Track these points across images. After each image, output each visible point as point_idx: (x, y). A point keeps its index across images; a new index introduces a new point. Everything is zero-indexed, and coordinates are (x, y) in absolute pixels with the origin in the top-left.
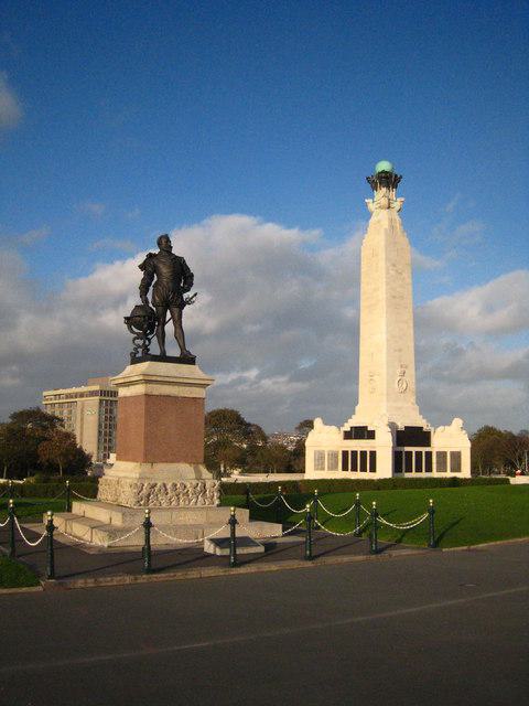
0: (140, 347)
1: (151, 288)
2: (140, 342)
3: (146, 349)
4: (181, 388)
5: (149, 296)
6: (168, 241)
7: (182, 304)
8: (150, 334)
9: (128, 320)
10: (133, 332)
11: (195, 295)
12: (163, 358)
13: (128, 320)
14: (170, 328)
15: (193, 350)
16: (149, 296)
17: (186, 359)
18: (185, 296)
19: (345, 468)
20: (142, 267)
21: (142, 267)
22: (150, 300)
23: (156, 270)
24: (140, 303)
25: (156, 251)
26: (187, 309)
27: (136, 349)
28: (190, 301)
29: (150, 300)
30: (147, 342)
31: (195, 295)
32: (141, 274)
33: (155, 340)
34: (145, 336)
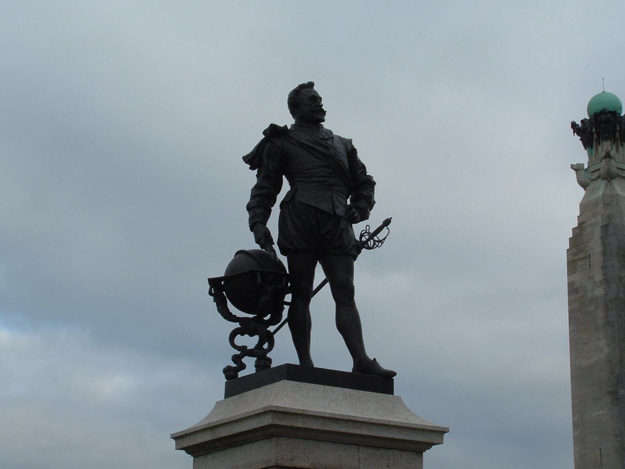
1: (276, 210)
2: (250, 341)
3: (260, 354)
5: (273, 225)
6: (316, 100)
8: (272, 322)
11: (387, 222)
12: (305, 372)
14: (323, 306)
16: (273, 225)
18: (358, 229)
20: (252, 160)
21: (252, 160)
22: (275, 234)
24: (250, 244)
25: (287, 120)
27: (236, 359)
28: (372, 240)
29: (275, 234)
30: (266, 346)
31: (387, 222)
32: (250, 178)
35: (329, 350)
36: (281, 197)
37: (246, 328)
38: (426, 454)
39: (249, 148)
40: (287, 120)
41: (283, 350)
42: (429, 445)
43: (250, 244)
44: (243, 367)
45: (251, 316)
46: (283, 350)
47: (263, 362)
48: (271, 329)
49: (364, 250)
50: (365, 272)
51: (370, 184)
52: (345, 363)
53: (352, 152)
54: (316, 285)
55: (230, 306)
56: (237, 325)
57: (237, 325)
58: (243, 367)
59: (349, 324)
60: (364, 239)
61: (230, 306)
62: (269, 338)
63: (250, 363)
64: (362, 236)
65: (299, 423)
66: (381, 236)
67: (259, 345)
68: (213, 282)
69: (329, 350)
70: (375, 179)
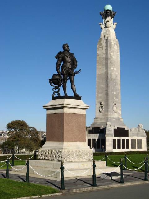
2: (57, 90)
3: (58, 92)
4: (52, 111)
9: (50, 80)
10: (52, 86)
11: (80, 70)
15: (78, 92)
17: (77, 97)
19: (114, 147)
21: (57, 57)
24: (56, 73)
25: (62, 50)
31: (80, 70)
32: (56, 61)
33: (61, 88)
34: (57, 88)
35: (70, 93)
37: (55, 88)
40: (62, 50)
43: (56, 73)
44: (55, 94)
45: (56, 86)
47: (59, 94)
49: (76, 75)
50: (76, 78)
52: (72, 95)
56: (54, 87)
57: (54, 87)
58: (55, 94)
61: (53, 84)
66: (79, 72)
68: (50, 80)
69: (70, 93)
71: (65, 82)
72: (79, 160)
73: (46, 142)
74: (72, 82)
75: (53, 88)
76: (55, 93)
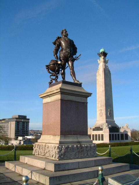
0: (54, 80)
1: (59, 52)
2: (54, 77)
3: (56, 80)
7: (73, 60)
10: (50, 73)
13: (48, 67)
14: (68, 71)
18: (74, 56)
20: (55, 43)
23: (60, 45)
24: (54, 58)
25: (60, 36)
26: (75, 62)
27: (51, 80)
35: (69, 78)
36: (59, 50)
38: (88, 98)
39: (54, 41)
41: (60, 78)
42: (89, 96)
43: (54, 58)
44: (52, 82)
46: (60, 78)
48: (58, 75)
51: (76, 48)
52: (72, 81)
53: (73, 42)
54: (66, 66)
55: (50, 70)
56: (51, 74)
58: (52, 82)
59: (73, 74)
60: (75, 58)
61: (50, 70)
62: (57, 77)
63: (54, 81)
64: (75, 58)
65: (66, 91)
67: (56, 78)
70: (77, 48)
71: (64, 68)
72: (80, 157)
73: (42, 137)
74: (72, 68)
75: (51, 76)
76: (53, 81)
